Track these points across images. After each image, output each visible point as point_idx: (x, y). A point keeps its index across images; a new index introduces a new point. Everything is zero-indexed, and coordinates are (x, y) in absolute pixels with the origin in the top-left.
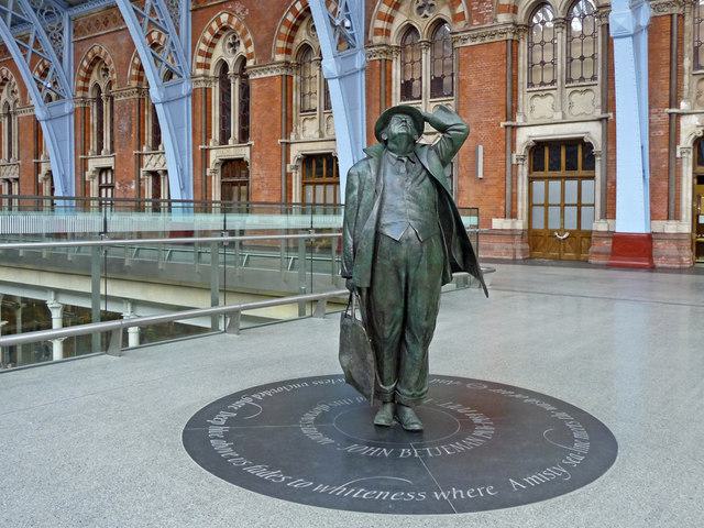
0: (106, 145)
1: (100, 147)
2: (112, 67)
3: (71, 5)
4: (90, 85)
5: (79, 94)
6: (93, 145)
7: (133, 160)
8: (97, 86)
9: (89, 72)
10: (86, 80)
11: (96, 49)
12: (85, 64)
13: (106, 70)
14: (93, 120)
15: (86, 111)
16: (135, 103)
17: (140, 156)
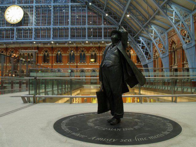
0: (176, 62)
1: (175, 63)
2: (176, 42)
3: (167, 30)
4: (172, 48)
5: (170, 51)
6: (173, 63)
7: (182, 65)
8: (173, 48)
9: (172, 45)
10: (171, 47)
11: (173, 39)
12: (171, 43)
13: (175, 44)
14: (173, 56)
15: (171, 54)
16: (181, 51)
17: (183, 65)
